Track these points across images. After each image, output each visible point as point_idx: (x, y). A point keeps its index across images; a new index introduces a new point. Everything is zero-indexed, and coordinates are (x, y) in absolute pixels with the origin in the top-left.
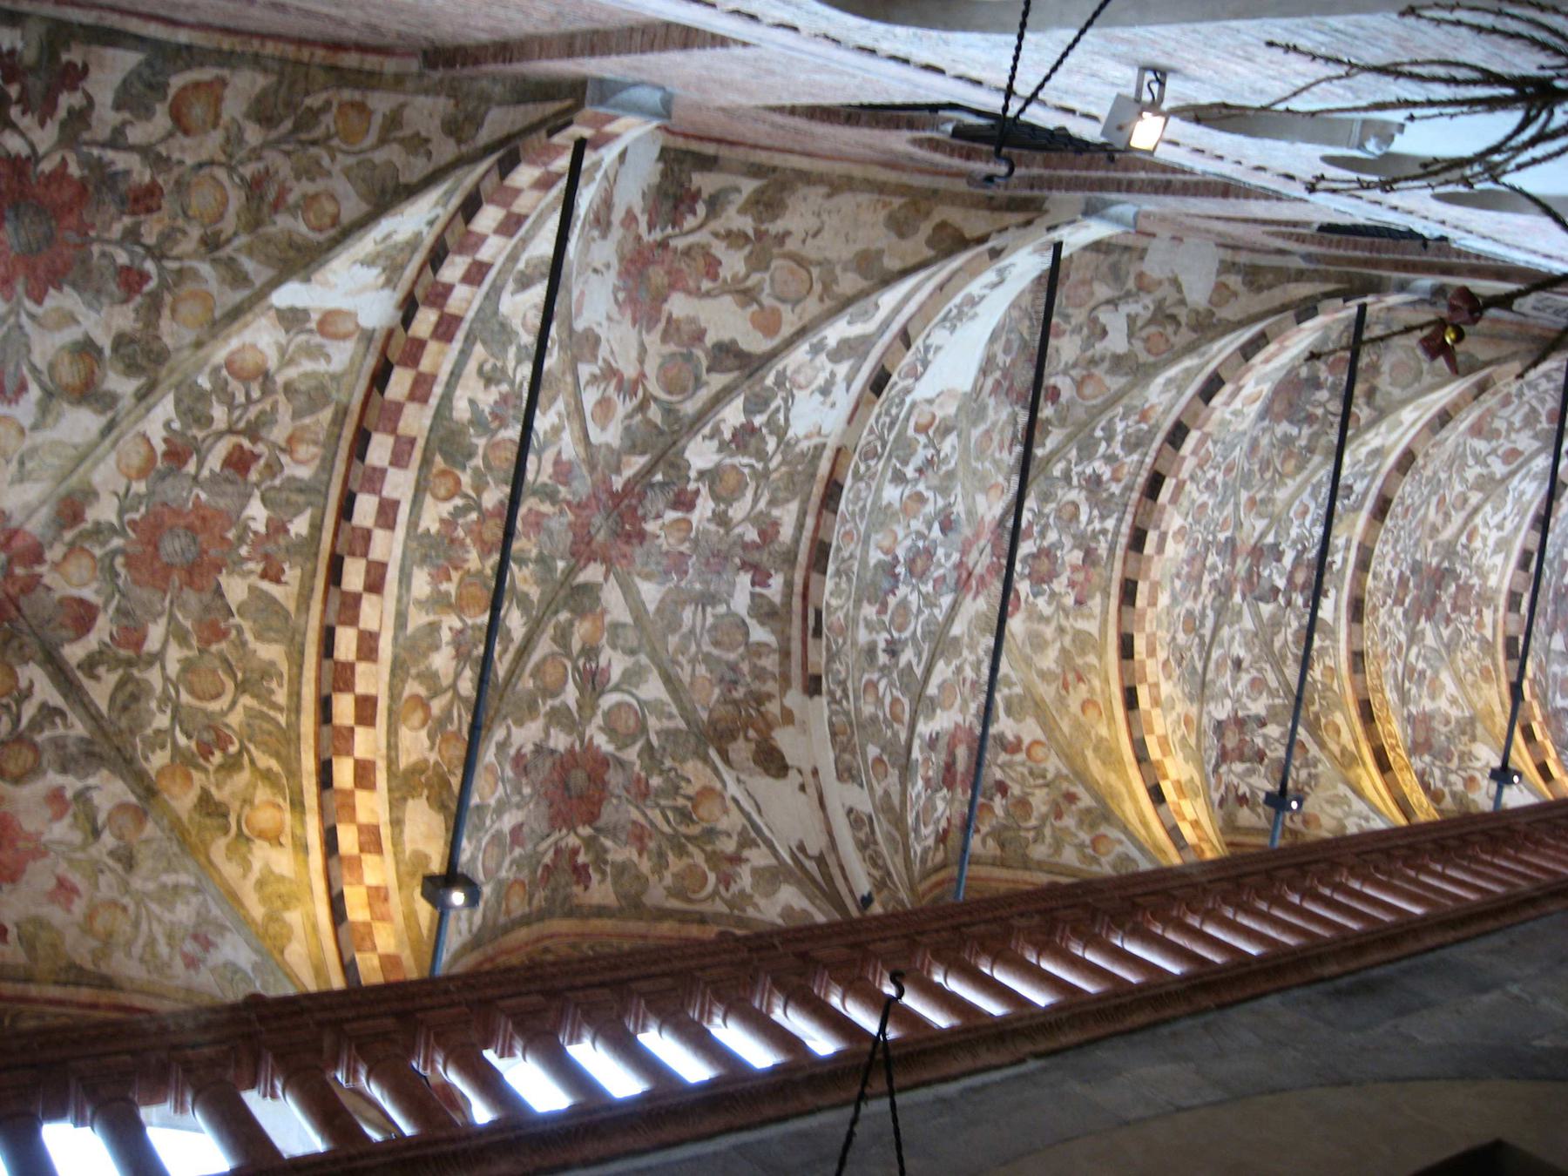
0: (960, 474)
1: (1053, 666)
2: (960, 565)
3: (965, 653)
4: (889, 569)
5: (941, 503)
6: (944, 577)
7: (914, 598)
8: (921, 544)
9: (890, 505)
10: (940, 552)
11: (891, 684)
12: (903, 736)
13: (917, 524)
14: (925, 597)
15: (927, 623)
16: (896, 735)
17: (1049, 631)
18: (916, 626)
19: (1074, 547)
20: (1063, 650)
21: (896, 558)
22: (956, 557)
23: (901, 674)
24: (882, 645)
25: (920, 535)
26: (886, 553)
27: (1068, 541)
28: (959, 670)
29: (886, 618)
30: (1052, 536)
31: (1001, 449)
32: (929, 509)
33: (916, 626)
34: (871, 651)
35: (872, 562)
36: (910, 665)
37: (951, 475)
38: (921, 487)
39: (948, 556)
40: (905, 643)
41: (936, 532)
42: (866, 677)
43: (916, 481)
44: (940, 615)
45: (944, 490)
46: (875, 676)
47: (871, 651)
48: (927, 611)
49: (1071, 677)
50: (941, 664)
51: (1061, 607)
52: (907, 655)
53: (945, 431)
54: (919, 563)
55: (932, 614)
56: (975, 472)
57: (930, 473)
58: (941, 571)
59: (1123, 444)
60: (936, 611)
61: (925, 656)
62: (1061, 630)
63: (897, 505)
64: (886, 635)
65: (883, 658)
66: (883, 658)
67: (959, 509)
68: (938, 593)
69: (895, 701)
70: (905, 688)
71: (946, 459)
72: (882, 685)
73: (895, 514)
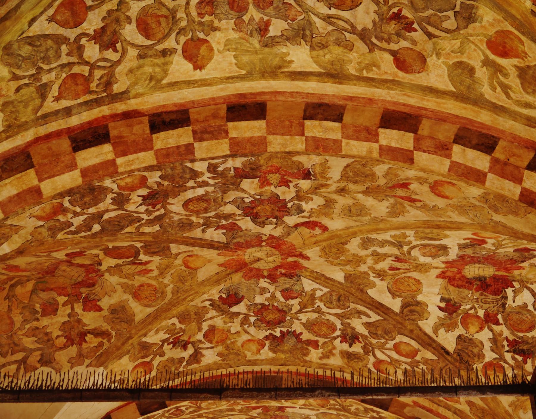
0: (181, 308)
1: (386, 203)
2: (272, 277)
3: (363, 268)
4: (276, 342)
5: (212, 313)
6: (283, 292)
7: (303, 317)
8: (252, 319)
9: (220, 354)
10: (259, 299)
11: (382, 347)
12: (430, 355)
13: (235, 326)
14: (303, 308)
15: (329, 303)
16: (426, 361)
17: (342, 201)
18: (332, 315)
19: (238, 188)
20: (367, 192)
21: (267, 338)
22: (264, 283)
23: (374, 335)
24: (345, 346)
25: (245, 320)
26: (263, 346)
27: (232, 195)
28: (381, 275)
29: (321, 341)
30: (229, 209)
31: (148, 271)
32: (219, 322)
33: (332, 315)
34: (348, 356)
35: (271, 355)
36: (368, 325)
37: (183, 318)
38: (200, 336)
39: (263, 291)
40: (347, 326)
41: (241, 308)
42: (370, 366)
43: (193, 344)
44: (322, 291)
45: (200, 315)
46: (372, 359)
47: (348, 356)
48: (318, 303)
49: (401, 192)
50: (371, 292)
51: (315, 190)
52: (358, 325)
53: (145, 347)
54: (270, 317)
55: (321, 299)
56: (176, 291)
57: (185, 338)
58: (279, 295)
59: (96, 202)
60: (318, 294)
61: (361, 308)
62: (342, 191)
63: (220, 348)
64: (337, 342)
65: (357, 348)
66: (357, 348)
67: (215, 293)
68: (300, 294)
69: (396, 348)
70: (388, 334)
71: (170, 330)
72: (380, 355)
73: (227, 348)
